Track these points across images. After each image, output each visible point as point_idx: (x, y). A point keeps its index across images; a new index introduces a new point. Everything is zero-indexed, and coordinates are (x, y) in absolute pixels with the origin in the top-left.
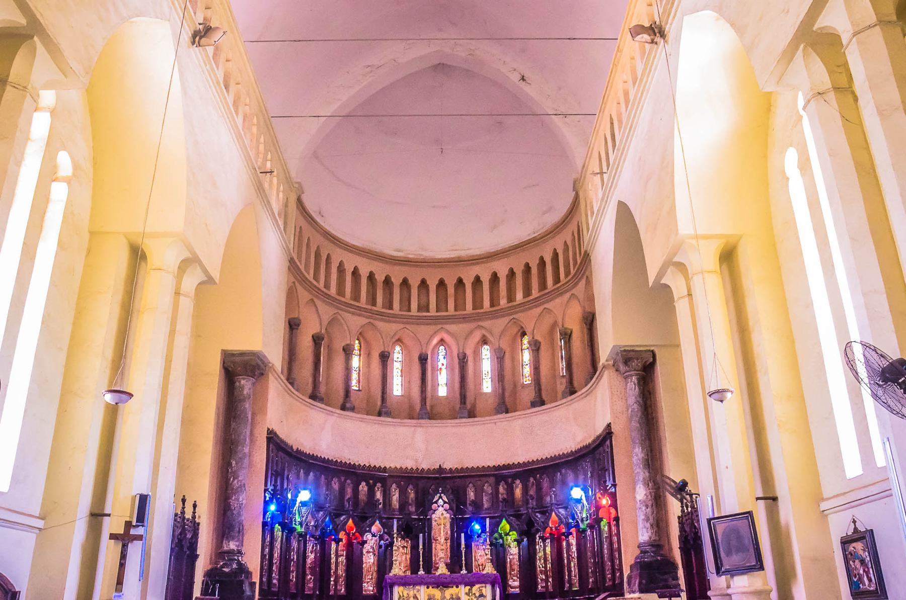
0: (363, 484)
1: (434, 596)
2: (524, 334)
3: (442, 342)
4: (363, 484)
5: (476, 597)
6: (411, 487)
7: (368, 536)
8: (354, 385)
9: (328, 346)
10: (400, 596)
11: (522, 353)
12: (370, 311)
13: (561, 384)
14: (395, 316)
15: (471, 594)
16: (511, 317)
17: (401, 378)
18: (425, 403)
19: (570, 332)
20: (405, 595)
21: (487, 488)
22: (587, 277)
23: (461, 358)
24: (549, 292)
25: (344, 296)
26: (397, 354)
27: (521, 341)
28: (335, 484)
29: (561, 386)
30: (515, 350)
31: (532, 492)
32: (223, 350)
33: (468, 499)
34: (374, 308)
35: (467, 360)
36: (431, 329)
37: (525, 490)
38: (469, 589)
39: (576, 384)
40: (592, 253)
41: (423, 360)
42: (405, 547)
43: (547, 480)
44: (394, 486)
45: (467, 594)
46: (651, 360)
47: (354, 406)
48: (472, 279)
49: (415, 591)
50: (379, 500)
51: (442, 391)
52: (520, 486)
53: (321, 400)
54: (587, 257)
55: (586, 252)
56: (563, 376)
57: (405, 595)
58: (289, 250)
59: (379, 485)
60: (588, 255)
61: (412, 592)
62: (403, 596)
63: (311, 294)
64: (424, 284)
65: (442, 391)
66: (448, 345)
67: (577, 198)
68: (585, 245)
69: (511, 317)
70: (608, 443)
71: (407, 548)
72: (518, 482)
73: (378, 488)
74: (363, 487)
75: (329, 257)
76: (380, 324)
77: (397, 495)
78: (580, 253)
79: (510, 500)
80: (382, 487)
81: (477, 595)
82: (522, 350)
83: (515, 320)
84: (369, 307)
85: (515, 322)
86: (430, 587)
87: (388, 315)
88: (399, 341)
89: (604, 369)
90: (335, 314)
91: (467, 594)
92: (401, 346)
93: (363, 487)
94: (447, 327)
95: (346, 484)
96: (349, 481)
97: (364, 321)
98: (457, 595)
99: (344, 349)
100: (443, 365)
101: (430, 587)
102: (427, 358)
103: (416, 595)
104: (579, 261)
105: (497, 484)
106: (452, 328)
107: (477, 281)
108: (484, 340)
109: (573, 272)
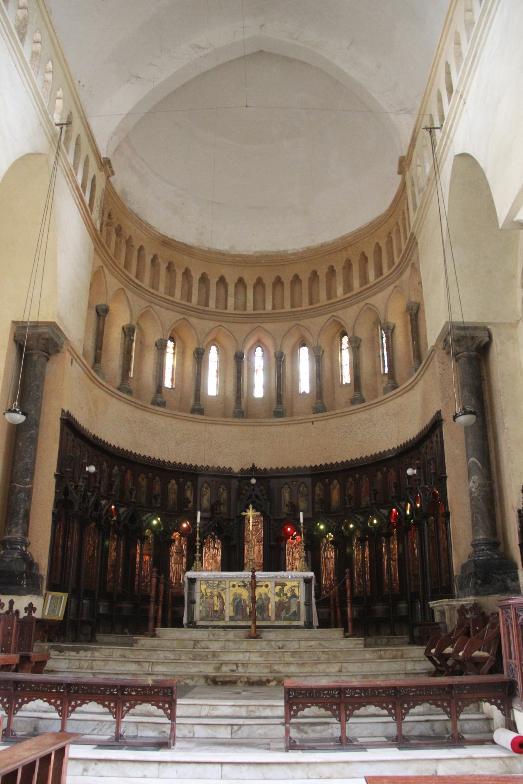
0: (173, 481)
1: (240, 595)
2: (344, 334)
3: (259, 343)
4: (173, 481)
5: (287, 597)
6: (223, 486)
7: (176, 535)
8: (168, 383)
9: (141, 342)
10: (203, 594)
11: (341, 353)
12: (185, 307)
13: (382, 382)
14: (212, 313)
15: (282, 595)
16: (331, 315)
17: (216, 378)
18: (240, 403)
19: (392, 325)
20: (209, 594)
21: (303, 489)
22: (413, 264)
23: (277, 355)
24: (370, 287)
25: (157, 290)
26: (213, 354)
27: (341, 341)
28: (143, 481)
29: (383, 383)
30: (335, 349)
31: (351, 491)
32: (14, 322)
33: (283, 502)
34: (188, 304)
35: (284, 360)
36: (247, 328)
37: (343, 490)
38: (280, 589)
39: (398, 379)
40: (419, 236)
41: (239, 358)
42: (216, 548)
43: (366, 480)
44: (206, 485)
45: (277, 594)
46: (487, 339)
47: (165, 402)
48: (291, 278)
49: (220, 589)
50: (189, 499)
51: (259, 392)
52: (338, 486)
53: (129, 392)
54: (413, 242)
55: (412, 234)
56: (384, 374)
57: (209, 594)
58: (95, 230)
59: (189, 483)
60: (415, 238)
61: (216, 590)
62: (206, 595)
63: (121, 282)
64: (241, 282)
65: (259, 392)
66: (265, 346)
67: (403, 186)
68: (412, 226)
69: (331, 315)
70: (438, 432)
71: (217, 549)
72: (335, 482)
73: (189, 487)
74: (173, 484)
75: (141, 248)
76: (193, 321)
77: (209, 494)
78: (406, 237)
79: (326, 500)
80: (192, 485)
81: (289, 595)
82: (341, 350)
83: (335, 318)
84: (184, 302)
85: (334, 320)
86: (237, 586)
87: (205, 312)
88: (215, 342)
89: (433, 352)
90: (148, 307)
91: (277, 594)
92: (217, 347)
93: (173, 484)
94: (264, 325)
95: (154, 481)
96: (157, 478)
97: (179, 316)
98: (266, 594)
99: (156, 345)
100: (260, 366)
101: (237, 586)
102: (243, 357)
103: (220, 593)
104: (404, 248)
105: (314, 486)
106: (269, 326)
107: (296, 279)
108: (303, 341)
109: (397, 261)
